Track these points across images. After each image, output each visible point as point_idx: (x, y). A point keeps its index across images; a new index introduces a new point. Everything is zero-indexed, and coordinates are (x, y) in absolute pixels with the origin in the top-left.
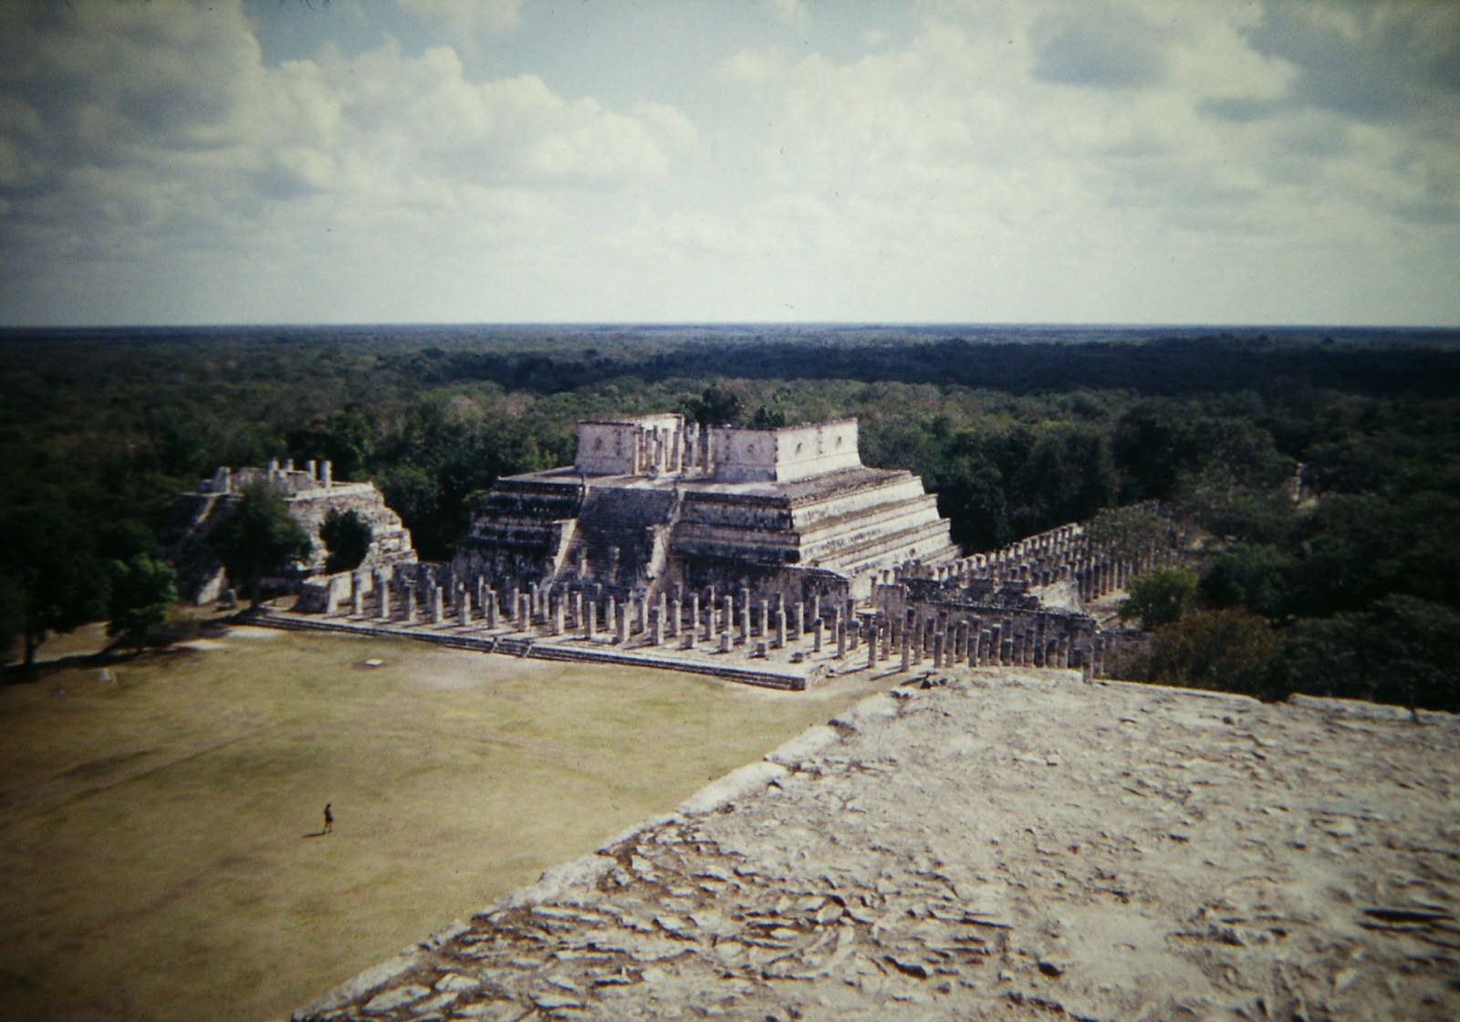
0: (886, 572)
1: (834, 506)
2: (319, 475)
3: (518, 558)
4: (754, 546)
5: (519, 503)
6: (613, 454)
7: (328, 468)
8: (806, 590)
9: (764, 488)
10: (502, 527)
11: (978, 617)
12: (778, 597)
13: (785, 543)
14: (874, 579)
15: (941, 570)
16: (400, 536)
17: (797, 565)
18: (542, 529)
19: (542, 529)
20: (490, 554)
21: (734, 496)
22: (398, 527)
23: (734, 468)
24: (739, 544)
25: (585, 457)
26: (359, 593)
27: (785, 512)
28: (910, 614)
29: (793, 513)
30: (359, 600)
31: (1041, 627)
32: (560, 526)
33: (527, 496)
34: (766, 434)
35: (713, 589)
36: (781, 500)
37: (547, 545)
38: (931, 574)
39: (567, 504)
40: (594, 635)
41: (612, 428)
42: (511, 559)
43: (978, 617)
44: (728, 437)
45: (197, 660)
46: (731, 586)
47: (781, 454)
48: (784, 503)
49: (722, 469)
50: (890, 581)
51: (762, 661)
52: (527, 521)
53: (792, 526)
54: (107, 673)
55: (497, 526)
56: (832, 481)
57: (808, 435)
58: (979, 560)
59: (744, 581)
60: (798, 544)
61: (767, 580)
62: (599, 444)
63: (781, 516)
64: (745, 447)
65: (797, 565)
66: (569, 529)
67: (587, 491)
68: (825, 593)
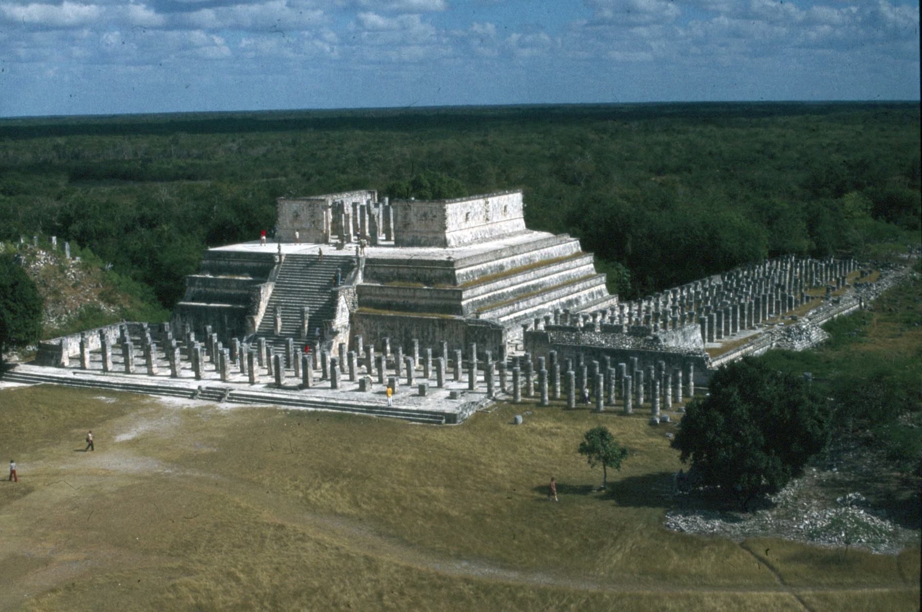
0: (537, 322)
12: (442, 345)
14: (525, 327)
26: (87, 350)
29: (457, 272)
30: (87, 356)
32: (259, 289)
34: (435, 205)
35: (388, 341)
37: (249, 302)
38: (577, 321)
39: (263, 267)
40: (284, 381)
41: (308, 203)
44: (405, 209)
47: (451, 222)
48: (449, 264)
57: (476, 204)
60: (461, 299)
62: (296, 216)
66: (267, 292)
67: (283, 258)
68: (483, 341)
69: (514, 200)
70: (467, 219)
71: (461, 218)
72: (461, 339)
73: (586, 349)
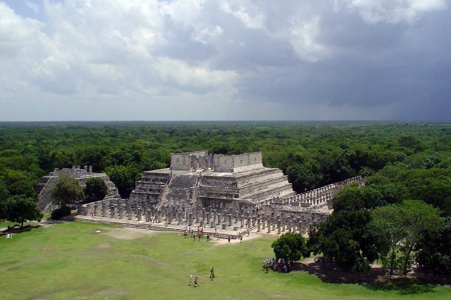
1: (252, 181)
2: (88, 171)
3: (151, 197)
4: (225, 193)
5: (151, 180)
6: (182, 164)
7: (91, 169)
8: (241, 207)
9: (229, 174)
10: (146, 188)
11: (293, 214)
13: (234, 192)
15: (285, 200)
16: (115, 190)
17: (238, 199)
18: (158, 188)
19: (158, 188)
20: (141, 197)
21: (219, 177)
22: (114, 188)
23: (220, 168)
24: (221, 192)
25: (173, 163)
27: (234, 182)
28: (273, 214)
31: (313, 218)
33: (154, 177)
36: (233, 178)
39: (166, 178)
41: (182, 155)
42: (148, 198)
43: (293, 214)
45: (46, 231)
46: (217, 206)
49: (216, 168)
50: (268, 204)
51: (224, 230)
52: (154, 186)
53: (237, 186)
54: (8, 236)
55: (144, 187)
56: (252, 172)
58: (298, 196)
59: (222, 204)
61: (228, 204)
63: (234, 184)
64: (224, 161)
65: (238, 199)
69: (259, 156)
70: (241, 162)
71: (239, 162)
72: (238, 207)
73: (284, 211)
